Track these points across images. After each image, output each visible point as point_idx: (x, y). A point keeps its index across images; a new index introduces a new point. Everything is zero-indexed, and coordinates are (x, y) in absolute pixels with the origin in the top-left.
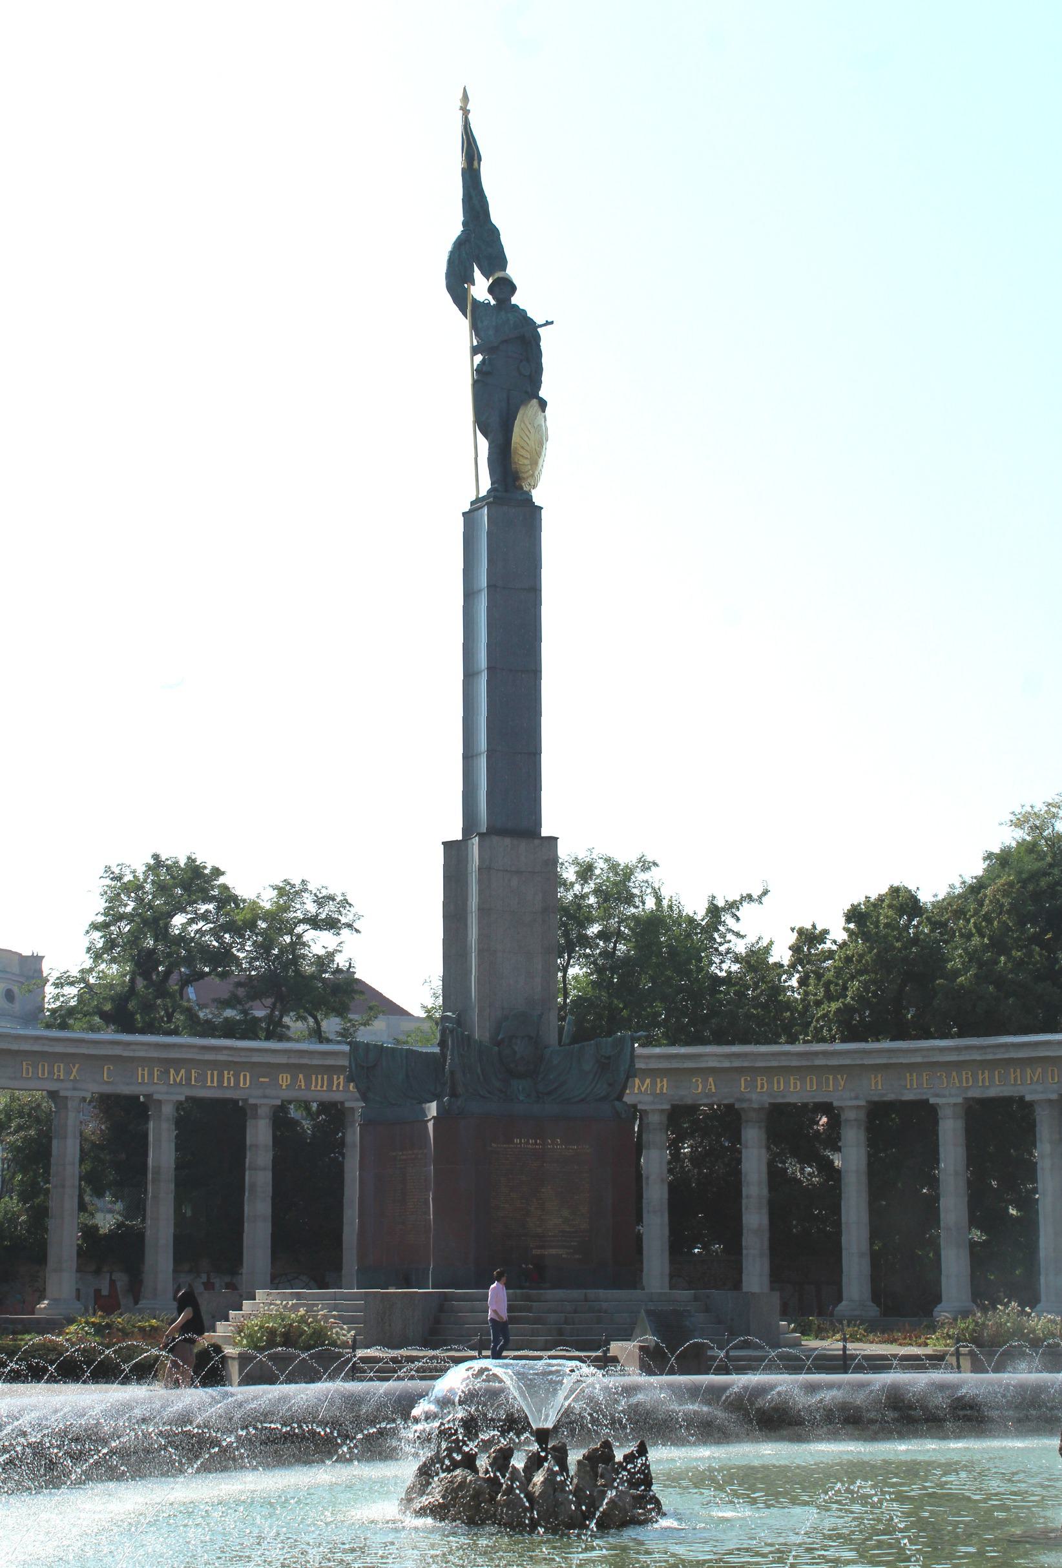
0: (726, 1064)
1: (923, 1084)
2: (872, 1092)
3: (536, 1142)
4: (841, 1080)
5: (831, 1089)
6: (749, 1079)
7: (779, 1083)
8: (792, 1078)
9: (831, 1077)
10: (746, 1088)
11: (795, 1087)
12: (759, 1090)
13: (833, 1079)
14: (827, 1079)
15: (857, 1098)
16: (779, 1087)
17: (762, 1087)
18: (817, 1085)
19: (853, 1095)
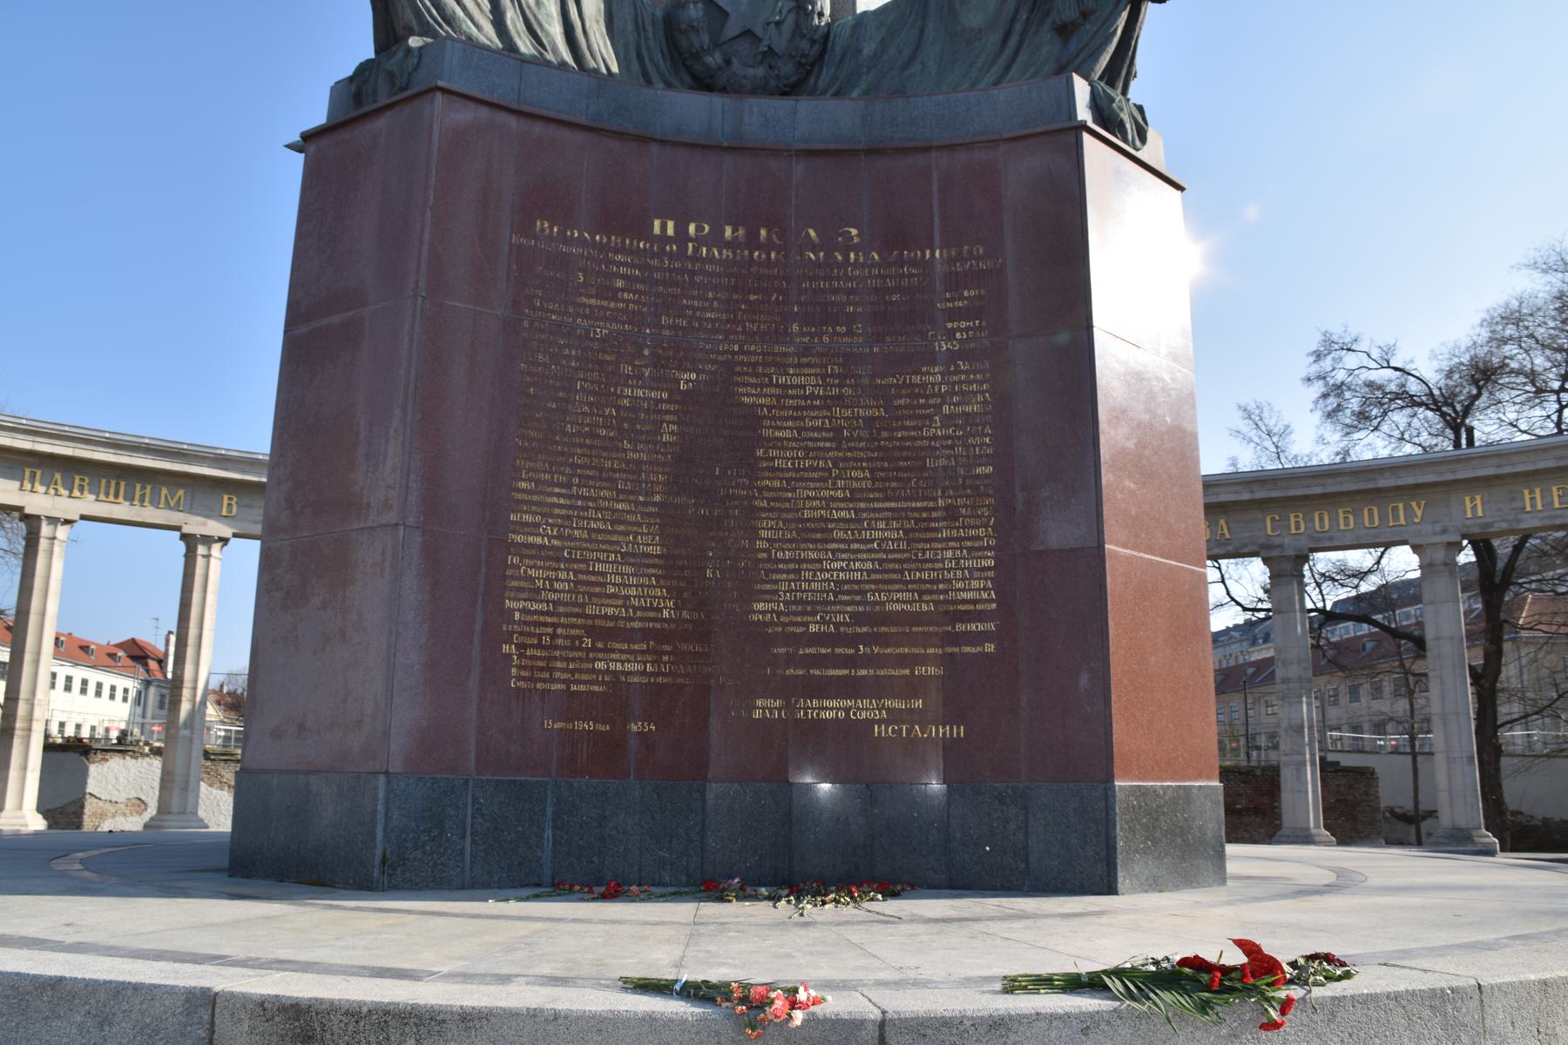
0: (1246, 496)
1: (1552, 503)
2: (1468, 522)
3: (752, 235)
4: (1416, 509)
5: (1402, 522)
6: (1277, 518)
7: (1321, 520)
8: (1341, 511)
9: (1401, 505)
10: (1273, 530)
11: (1347, 524)
12: (1293, 531)
13: (1405, 509)
14: (1395, 509)
15: (1444, 531)
16: (1322, 526)
17: (1298, 528)
18: (1380, 519)
19: (1438, 528)
